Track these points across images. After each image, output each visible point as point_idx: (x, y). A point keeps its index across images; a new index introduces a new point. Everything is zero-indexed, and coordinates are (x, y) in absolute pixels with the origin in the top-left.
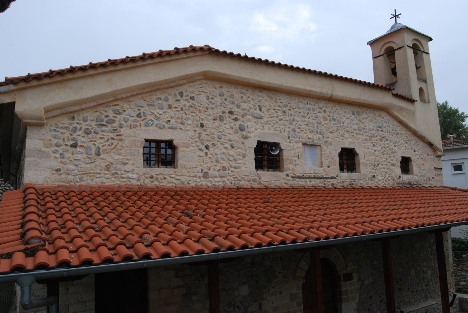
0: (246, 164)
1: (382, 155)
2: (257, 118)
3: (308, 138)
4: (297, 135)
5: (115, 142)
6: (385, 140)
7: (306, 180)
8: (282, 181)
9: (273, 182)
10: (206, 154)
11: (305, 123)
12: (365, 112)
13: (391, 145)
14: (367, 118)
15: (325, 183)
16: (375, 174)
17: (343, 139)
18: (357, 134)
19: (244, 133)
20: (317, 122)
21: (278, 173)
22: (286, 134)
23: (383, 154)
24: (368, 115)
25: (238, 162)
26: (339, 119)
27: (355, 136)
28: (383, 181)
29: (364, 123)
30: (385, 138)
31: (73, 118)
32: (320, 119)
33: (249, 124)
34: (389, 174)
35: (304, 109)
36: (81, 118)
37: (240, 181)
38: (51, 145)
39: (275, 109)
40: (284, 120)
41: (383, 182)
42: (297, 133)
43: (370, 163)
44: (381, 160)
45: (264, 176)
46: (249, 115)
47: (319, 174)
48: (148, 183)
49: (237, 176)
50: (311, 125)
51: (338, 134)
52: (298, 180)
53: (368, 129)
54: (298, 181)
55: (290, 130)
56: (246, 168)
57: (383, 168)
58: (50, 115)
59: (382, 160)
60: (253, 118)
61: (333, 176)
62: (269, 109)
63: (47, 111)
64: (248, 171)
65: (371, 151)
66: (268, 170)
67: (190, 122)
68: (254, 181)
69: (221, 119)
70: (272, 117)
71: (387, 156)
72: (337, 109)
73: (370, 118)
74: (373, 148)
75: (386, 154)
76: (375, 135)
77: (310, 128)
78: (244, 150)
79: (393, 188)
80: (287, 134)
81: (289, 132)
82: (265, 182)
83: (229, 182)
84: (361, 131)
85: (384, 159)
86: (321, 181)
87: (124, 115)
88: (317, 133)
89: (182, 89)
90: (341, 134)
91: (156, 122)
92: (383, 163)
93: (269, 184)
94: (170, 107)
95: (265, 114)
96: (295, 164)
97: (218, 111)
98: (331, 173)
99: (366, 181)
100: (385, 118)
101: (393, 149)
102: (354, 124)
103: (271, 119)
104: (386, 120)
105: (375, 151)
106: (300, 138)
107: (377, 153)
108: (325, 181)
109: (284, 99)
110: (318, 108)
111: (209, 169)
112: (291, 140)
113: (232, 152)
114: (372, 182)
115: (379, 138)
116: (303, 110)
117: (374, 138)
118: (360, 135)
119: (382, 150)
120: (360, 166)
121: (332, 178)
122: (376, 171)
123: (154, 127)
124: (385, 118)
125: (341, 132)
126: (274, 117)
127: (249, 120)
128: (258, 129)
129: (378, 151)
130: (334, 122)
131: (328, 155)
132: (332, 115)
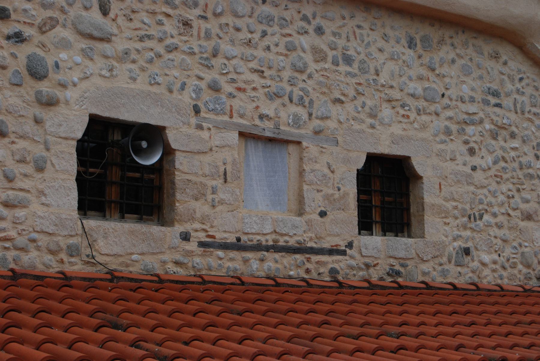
0: (45, 195)
1: (494, 184)
2: (91, 37)
3: (262, 117)
4: (224, 103)
6: (508, 137)
7: (249, 255)
8: (166, 257)
9: (134, 257)
11: (253, 65)
12: (449, 41)
13: (526, 154)
14: (453, 61)
15: (308, 266)
16: (470, 244)
17: (373, 127)
18: (419, 112)
19: (44, 87)
20: (293, 65)
21: (156, 230)
23: (499, 179)
24: (458, 51)
25: (19, 183)
26: (366, 59)
27: (412, 118)
28: (494, 266)
29: (444, 76)
30: (505, 129)
32: (302, 54)
33: (63, 56)
34: (515, 244)
35: (250, 17)
37: (22, 249)
39: (154, 13)
40: (184, 52)
41: (494, 271)
42: (224, 97)
43: (456, 208)
44: (490, 199)
45: (105, 236)
46: (64, 26)
47: (291, 236)
49: (13, 233)
50: (273, 72)
51: (360, 109)
52: (220, 253)
53: (454, 97)
54: (221, 259)
55: (203, 85)
56: (45, 209)
57: (496, 224)
59: (493, 200)
60: (78, 37)
61: (336, 246)
62: (133, 12)
64: (53, 217)
65: (461, 168)
66: (123, 217)
68: (73, 251)
70: (141, 39)
71: (511, 186)
72: (359, 27)
73: (463, 62)
74: (468, 158)
75: (508, 180)
76: (476, 118)
77: (269, 82)
78: (42, 146)
79: (525, 290)
80: (191, 98)
81: (198, 91)
82: (108, 259)
84: (432, 101)
85: (501, 198)
86: (296, 260)
88: (291, 101)
90: (367, 109)
92: (496, 209)
93: (121, 264)
95: (119, 27)
96: (213, 200)
98: (329, 235)
99: (441, 265)
100: (511, 64)
101: (530, 167)
102: (410, 79)
103: (139, 45)
104: (515, 73)
105: (472, 170)
106: (235, 115)
107: (479, 176)
108: (309, 260)
110: (297, 17)
112: (205, 118)
114: (459, 269)
115: (488, 126)
116: (247, 20)
117: (473, 127)
118: (430, 114)
119: (497, 167)
120: (424, 216)
121: (331, 252)
122: (475, 234)
124: (511, 64)
125: (369, 103)
126: (149, 37)
127: (65, 45)
128: (91, 74)
129: (484, 170)
130: (348, 69)
131: (324, 176)
132: (341, 43)
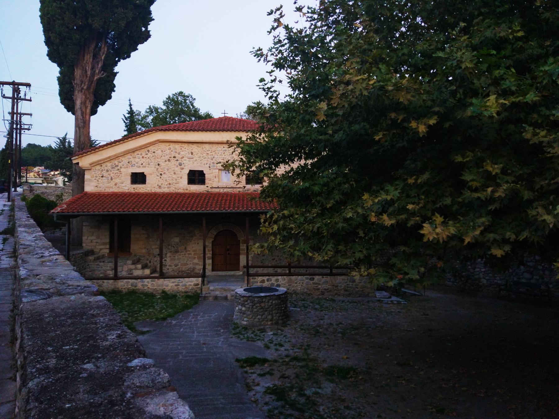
5: (118, 174)
10: (161, 177)
19: (181, 167)
22: (208, 165)
31: (102, 166)
36: (104, 165)
38: (94, 177)
48: (132, 191)
58: (93, 165)
63: (90, 164)
67: (152, 164)
68: (187, 189)
69: (169, 160)
81: (210, 164)
83: (172, 190)
87: (122, 163)
89: (149, 148)
91: (136, 165)
94: (143, 157)
97: (167, 158)
109: (207, 146)
111: (162, 184)
113: (174, 176)
123: (135, 167)
127: (185, 160)
